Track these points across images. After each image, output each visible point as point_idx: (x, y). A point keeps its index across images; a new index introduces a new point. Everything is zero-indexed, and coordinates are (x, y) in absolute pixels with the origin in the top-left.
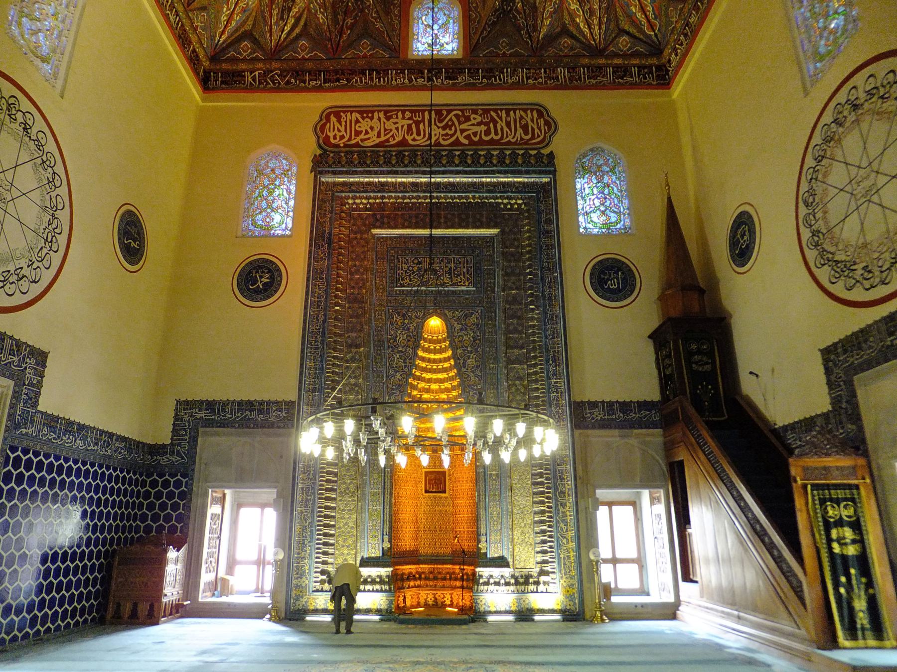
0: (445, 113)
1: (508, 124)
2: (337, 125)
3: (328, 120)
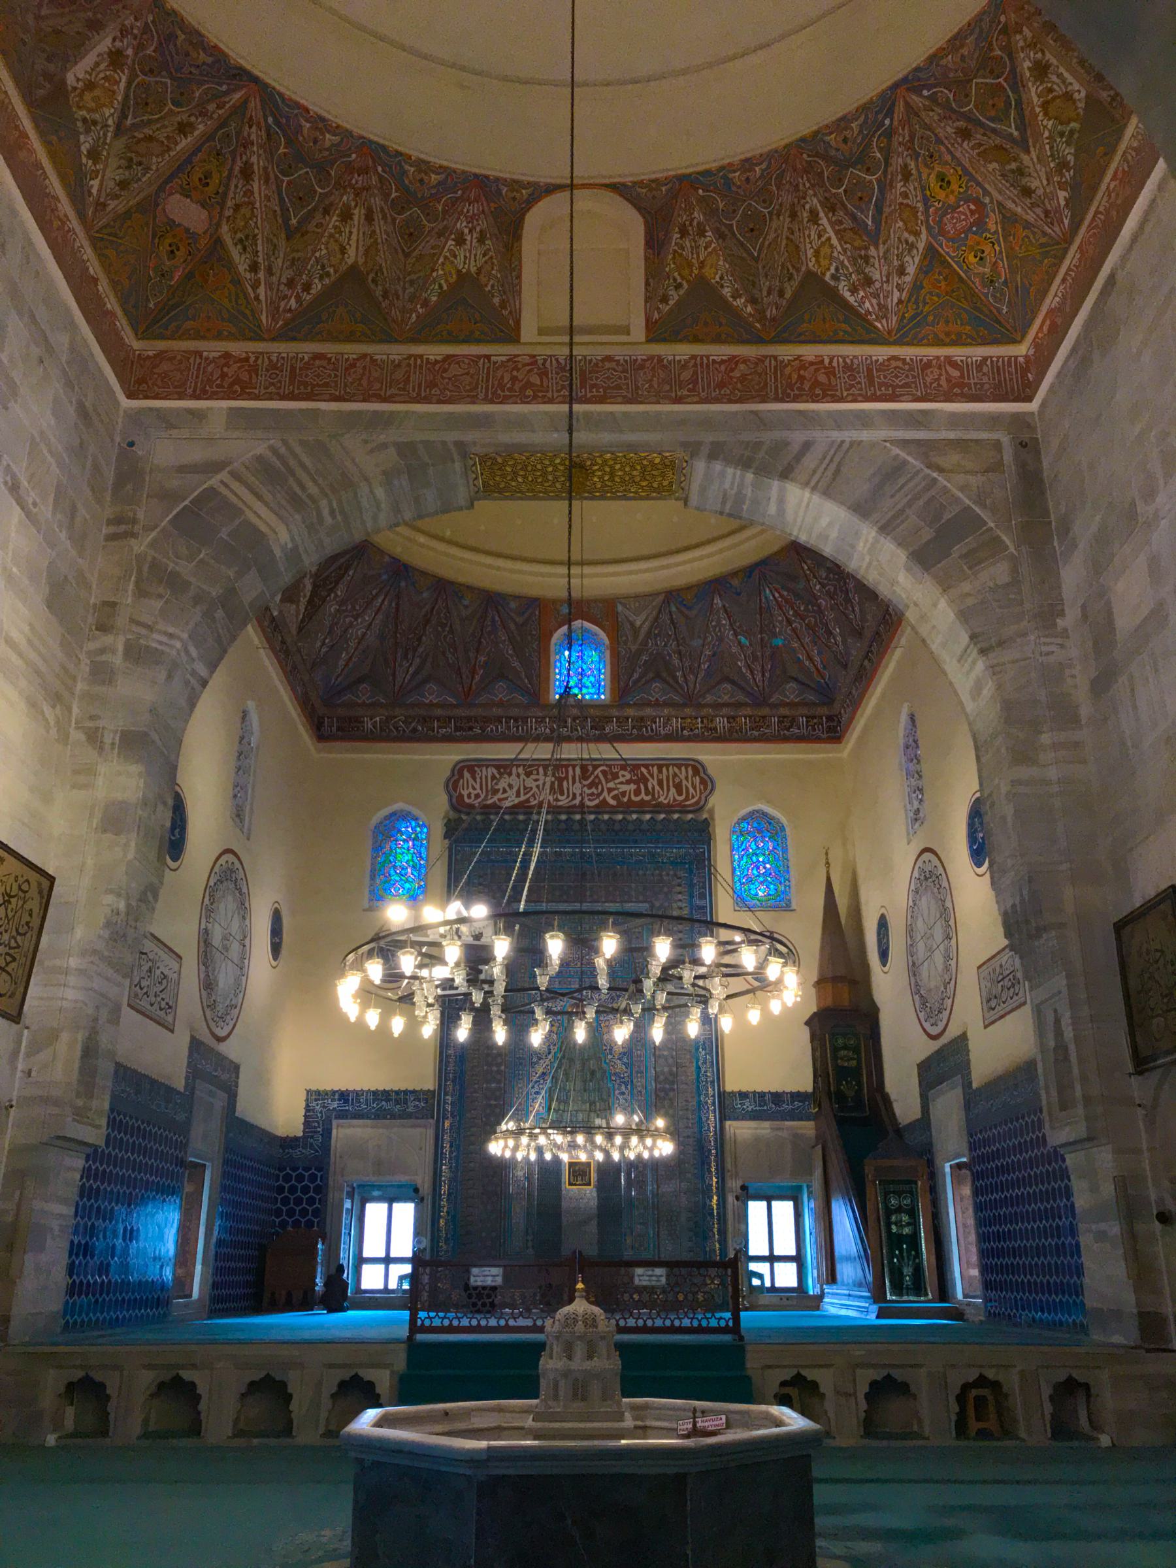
0: (590, 768)
1: (660, 783)
2: (471, 781)
3: (461, 776)
